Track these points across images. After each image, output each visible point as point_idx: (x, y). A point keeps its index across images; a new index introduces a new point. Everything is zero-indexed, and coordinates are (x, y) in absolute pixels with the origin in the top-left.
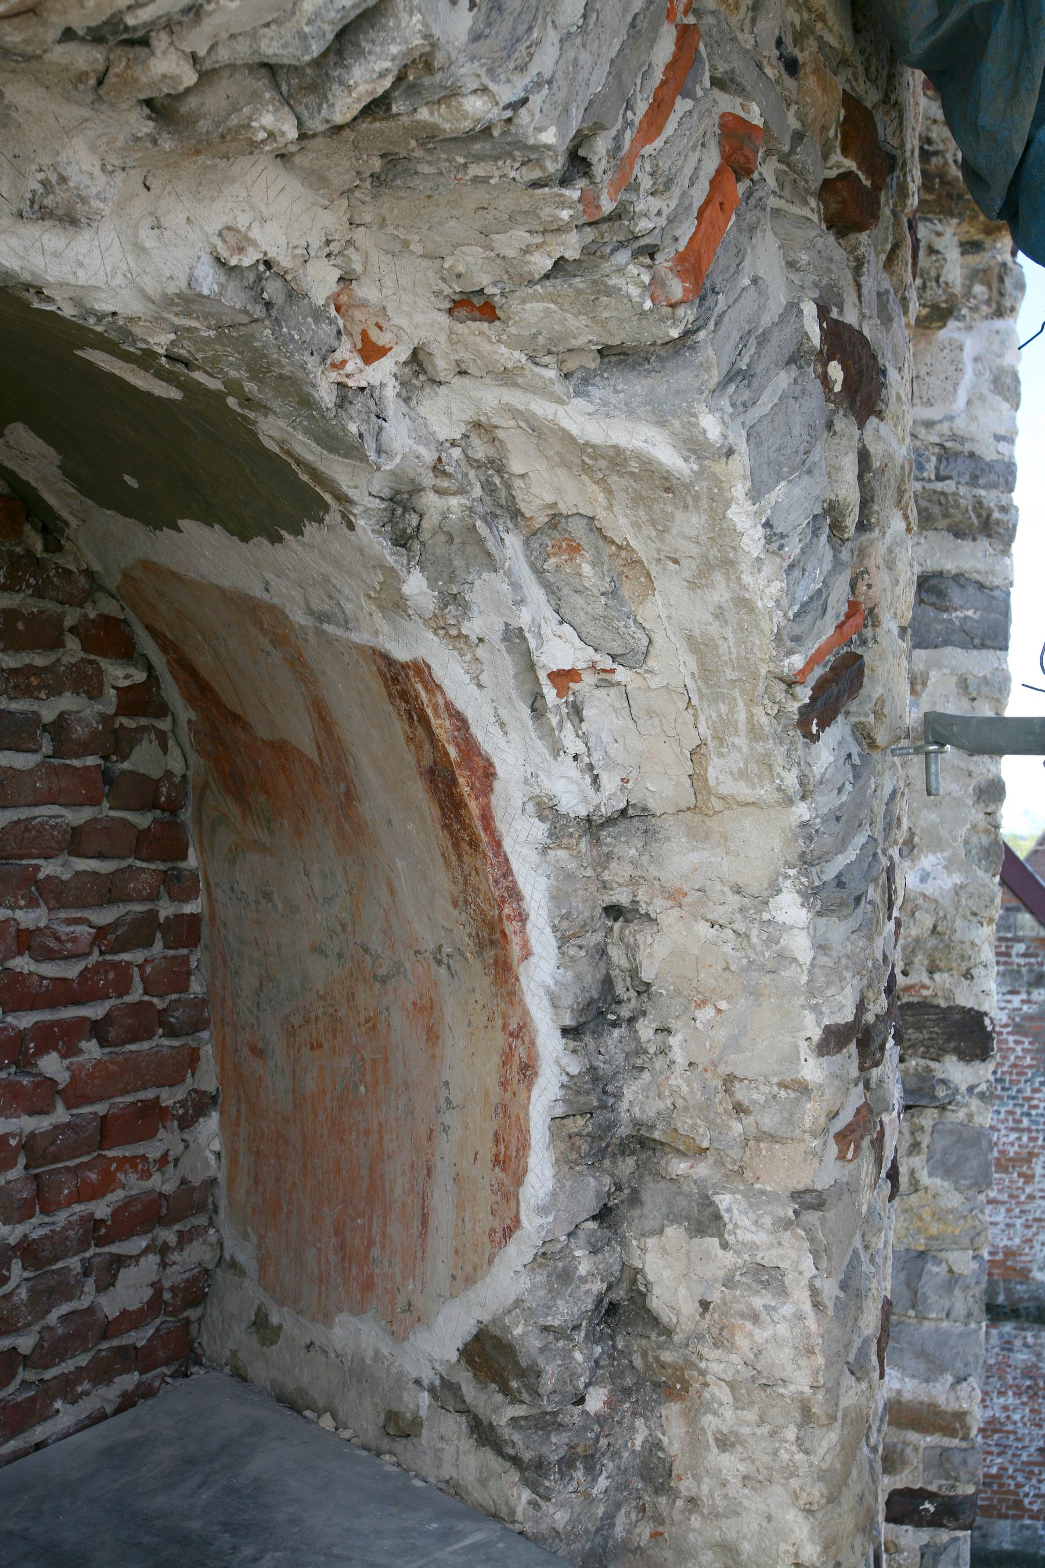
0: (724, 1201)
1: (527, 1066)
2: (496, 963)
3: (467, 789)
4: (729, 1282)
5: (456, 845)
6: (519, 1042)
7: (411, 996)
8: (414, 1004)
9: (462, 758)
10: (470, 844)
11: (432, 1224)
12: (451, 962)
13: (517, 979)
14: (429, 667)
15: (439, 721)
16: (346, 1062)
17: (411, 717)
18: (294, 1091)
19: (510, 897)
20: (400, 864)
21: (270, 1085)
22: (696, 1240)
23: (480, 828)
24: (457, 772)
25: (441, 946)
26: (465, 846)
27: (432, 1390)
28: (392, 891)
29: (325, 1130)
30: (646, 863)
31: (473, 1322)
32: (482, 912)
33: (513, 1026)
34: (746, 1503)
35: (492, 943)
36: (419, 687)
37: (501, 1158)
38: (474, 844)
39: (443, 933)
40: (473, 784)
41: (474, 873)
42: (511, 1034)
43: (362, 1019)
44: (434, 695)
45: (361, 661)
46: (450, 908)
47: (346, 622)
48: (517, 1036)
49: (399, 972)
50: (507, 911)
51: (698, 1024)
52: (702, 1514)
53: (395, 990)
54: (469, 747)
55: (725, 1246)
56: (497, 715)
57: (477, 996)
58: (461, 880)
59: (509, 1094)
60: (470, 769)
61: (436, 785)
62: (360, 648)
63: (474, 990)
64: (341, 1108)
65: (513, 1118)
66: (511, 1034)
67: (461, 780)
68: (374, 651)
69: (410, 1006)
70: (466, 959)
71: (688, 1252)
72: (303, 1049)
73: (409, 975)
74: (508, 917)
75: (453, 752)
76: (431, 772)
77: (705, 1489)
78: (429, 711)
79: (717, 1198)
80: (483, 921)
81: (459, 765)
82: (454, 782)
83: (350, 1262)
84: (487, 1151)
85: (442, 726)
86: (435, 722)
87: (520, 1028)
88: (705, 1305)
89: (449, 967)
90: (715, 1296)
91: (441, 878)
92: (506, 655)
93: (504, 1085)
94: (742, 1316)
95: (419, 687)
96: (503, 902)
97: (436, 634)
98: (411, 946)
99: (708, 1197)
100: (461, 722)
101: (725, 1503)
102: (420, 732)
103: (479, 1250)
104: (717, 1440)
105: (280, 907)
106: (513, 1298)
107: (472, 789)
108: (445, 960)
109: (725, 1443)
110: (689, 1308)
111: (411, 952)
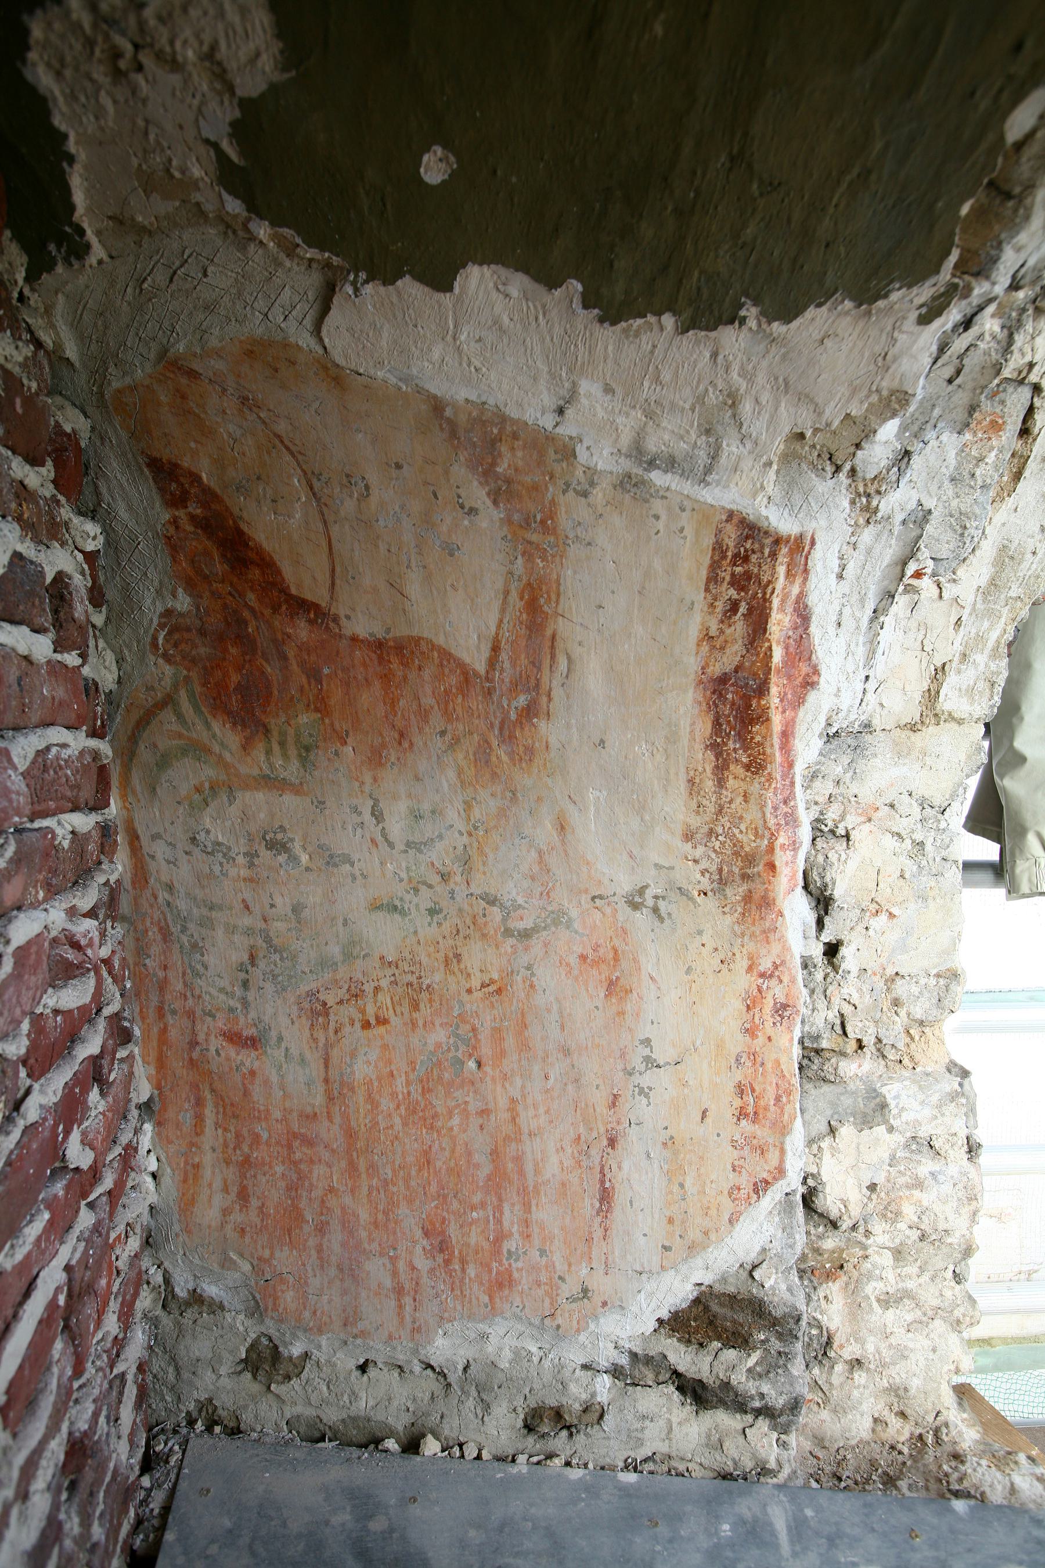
0: (890, 1091)
1: (785, 1006)
2: (748, 898)
3: (777, 700)
4: (893, 1161)
5: (721, 769)
6: (774, 982)
7: (578, 949)
8: (583, 958)
9: (785, 663)
10: (747, 767)
11: (620, 1198)
12: (662, 904)
13: (781, 914)
14: (813, 543)
15: (780, 616)
16: (439, 1035)
17: (734, 607)
18: (326, 1081)
19: (787, 824)
20: (592, 795)
21: (274, 1079)
22: (866, 1132)
23: (777, 746)
24: (774, 678)
25: (646, 887)
26: (737, 769)
27: (616, 1372)
28: (562, 827)
29: (397, 1120)
30: (848, 781)
31: (689, 1287)
32: (737, 844)
33: (766, 965)
34: (911, 1345)
35: (745, 877)
36: (781, 570)
37: (750, 1110)
38: (756, 766)
39: (653, 872)
40: (785, 694)
41: (740, 799)
42: (762, 975)
43: (476, 983)
44: (792, 583)
45: (689, 532)
46: (678, 842)
47: (708, 470)
48: (771, 976)
49: (556, 923)
50: (782, 839)
51: (871, 932)
52: (868, 1370)
53: (546, 945)
54: (801, 648)
55: (891, 1129)
56: (841, 614)
57: (705, 939)
58: (712, 808)
59: (761, 1040)
60: (789, 677)
61: (721, 696)
62: (703, 512)
63: (700, 933)
64: (426, 1091)
65: (769, 1065)
66: (762, 975)
67: (774, 690)
68: (731, 515)
69: (573, 960)
70: (691, 899)
71: (858, 1144)
72: (347, 1029)
73: (576, 925)
74: (783, 846)
75: (778, 655)
76: (723, 679)
77: (870, 1348)
78: (776, 602)
79: (884, 1090)
80: (736, 854)
81: (778, 671)
82: (762, 690)
83: (463, 1262)
84: (725, 1105)
85: (780, 622)
86: (775, 616)
87: (776, 967)
88: (872, 1187)
89: (656, 910)
90: (880, 1179)
91: (676, 808)
92: (893, 542)
93: (751, 1032)
94: (908, 1187)
95: (781, 570)
96: (778, 831)
97: (853, 502)
98: (586, 891)
99: (875, 1090)
100: (803, 616)
101: (892, 1352)
102: (739, 628)
103: (713, 1212)
104: (878, 1300)
105: (304, 858)
106: (758, 1249)
107: (782, 701)
108: (650, 902)
109: (886, 1301)
110: (855, 1196)
111: (585, 899)
